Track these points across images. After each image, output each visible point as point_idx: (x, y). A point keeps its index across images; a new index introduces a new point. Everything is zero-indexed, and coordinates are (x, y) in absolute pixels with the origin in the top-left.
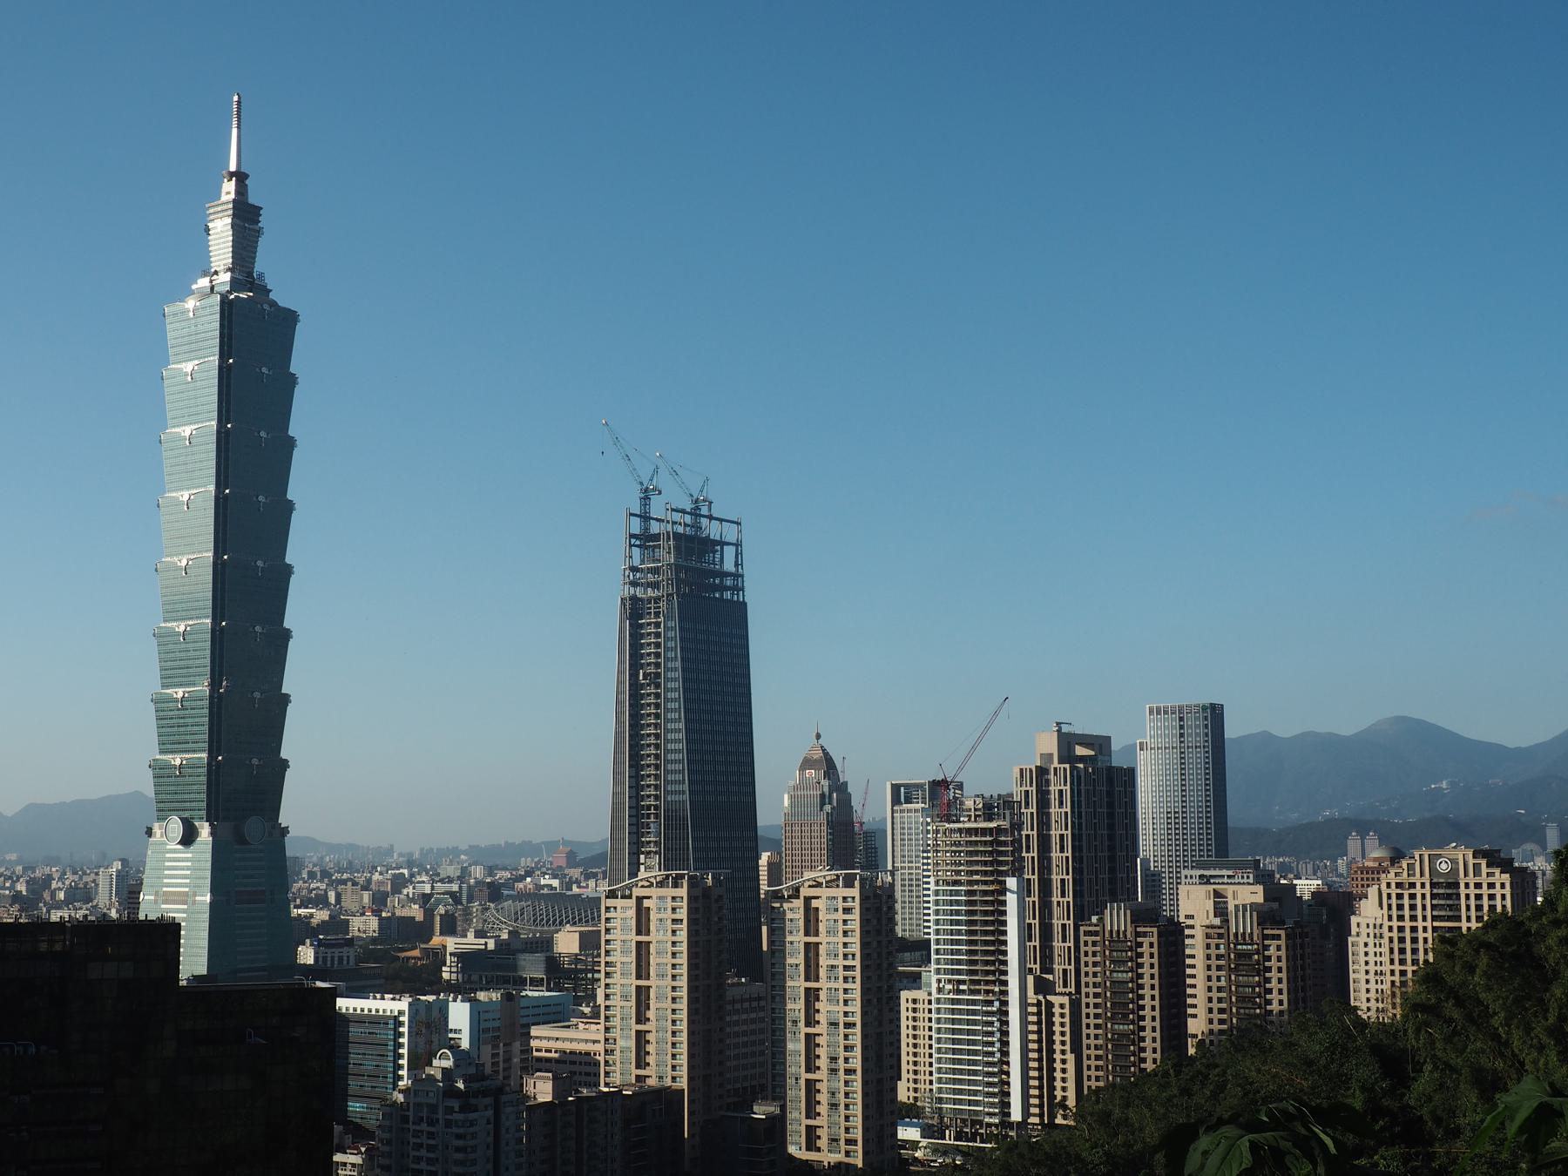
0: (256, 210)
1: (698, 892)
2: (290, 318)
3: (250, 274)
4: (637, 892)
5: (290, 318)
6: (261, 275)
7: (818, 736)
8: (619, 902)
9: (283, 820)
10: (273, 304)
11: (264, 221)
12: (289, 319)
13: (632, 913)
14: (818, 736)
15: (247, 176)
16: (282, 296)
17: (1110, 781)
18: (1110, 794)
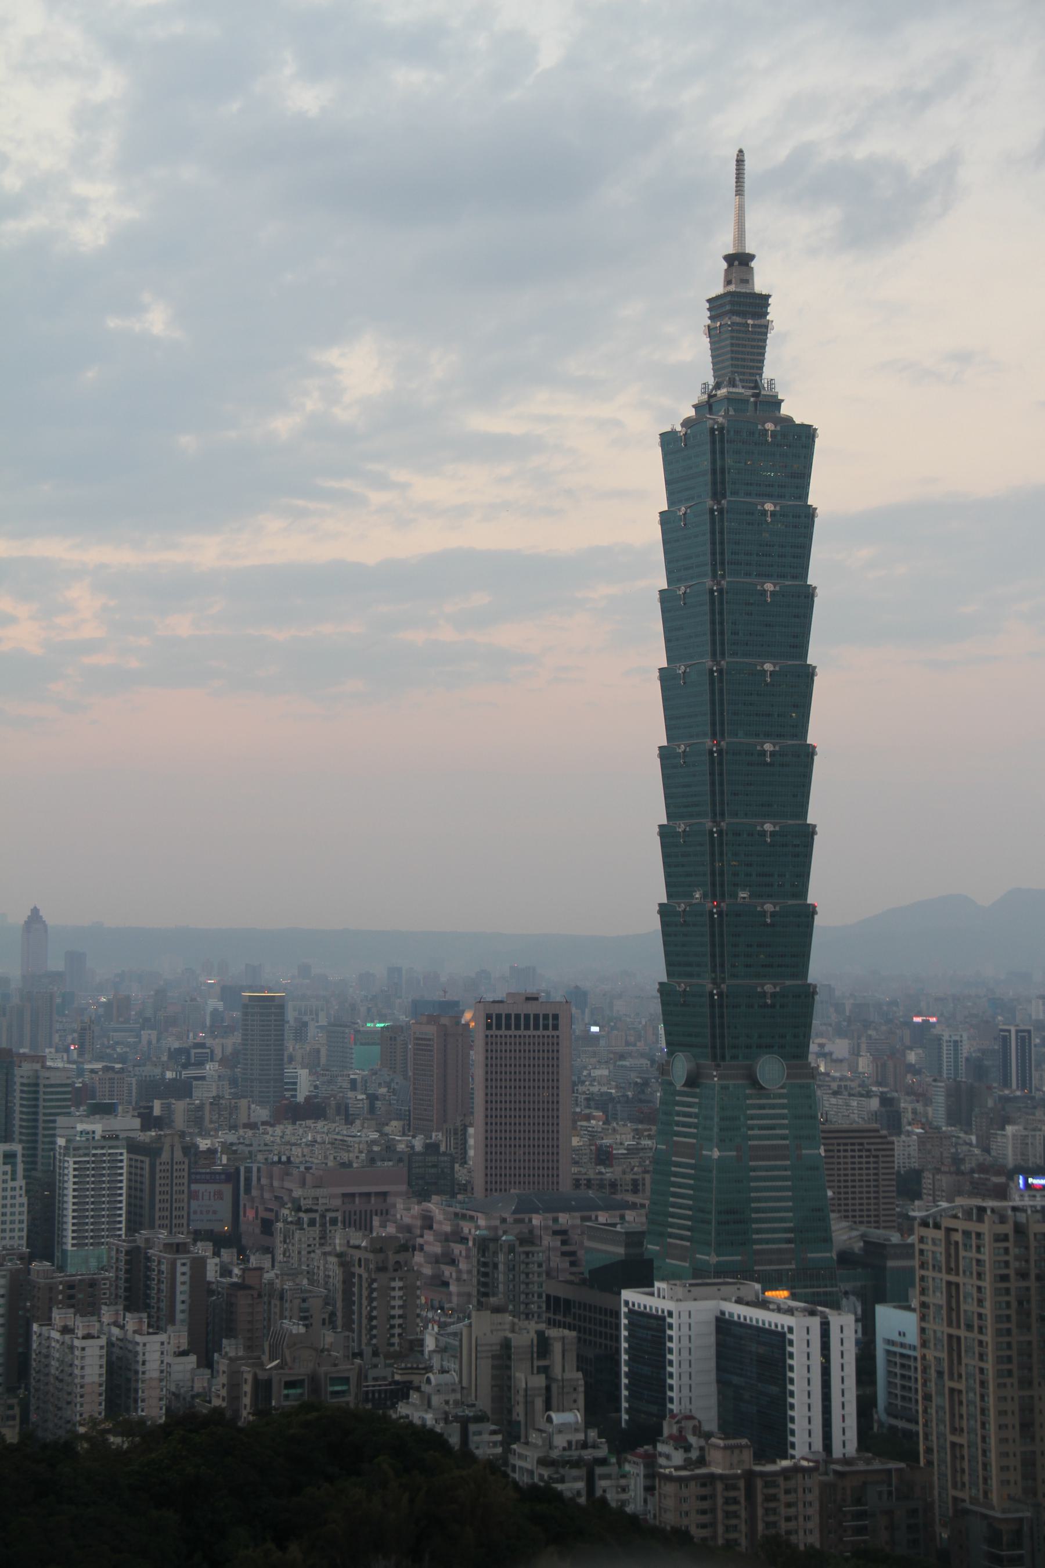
0: (763, 300)
1: (1008, 1229)
2: (805, 436)
3: (756, 385)
4: (946, 1223)
5: (805, 436)
6: (771, 382)
8: (930, 1233)
10: (789, 420)
11: (774, 313)
12: (802, 438)
13: (941, 1249)
15: (752, 257)
16: (795, 408)
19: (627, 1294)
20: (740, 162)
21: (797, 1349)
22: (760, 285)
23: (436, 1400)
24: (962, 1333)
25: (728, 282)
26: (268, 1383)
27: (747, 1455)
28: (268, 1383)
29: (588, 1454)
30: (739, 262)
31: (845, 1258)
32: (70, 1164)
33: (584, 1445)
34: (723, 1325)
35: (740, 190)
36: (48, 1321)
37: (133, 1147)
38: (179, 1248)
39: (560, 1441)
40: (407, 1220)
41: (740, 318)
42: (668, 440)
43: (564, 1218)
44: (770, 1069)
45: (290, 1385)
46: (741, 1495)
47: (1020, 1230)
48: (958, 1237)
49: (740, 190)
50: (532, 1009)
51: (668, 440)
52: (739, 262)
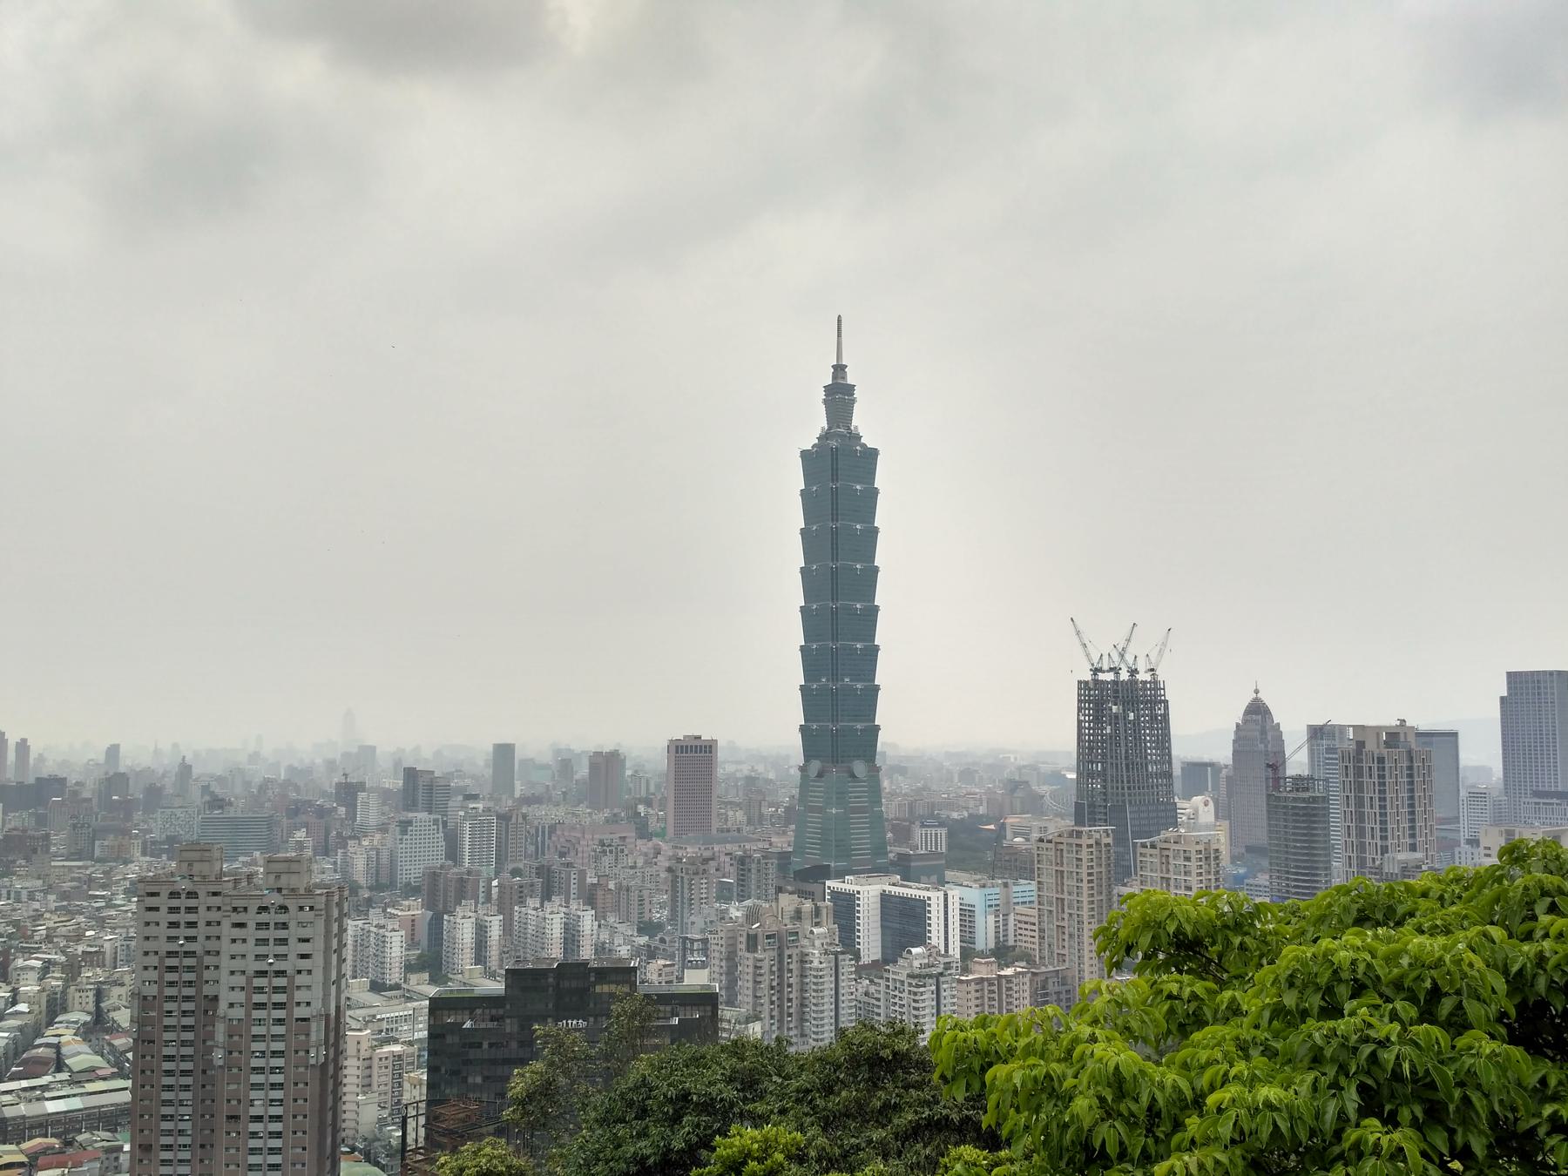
5: (873, 454)
7: (1257, 692)
8: (1044, 845)
9: (878, 762)
12: (873, 454)
14: (1257, 692)
16: (868, 440)
17: (1411, 759)
18: (1410, 768)
19: (828, 883)
20: (839, 321)
21: (933, 909)
22: (850, 381)
23: (817, 943)
24: (1065, 896)
25: (834, 377)
26: (756, 936)
27: (995, 967)
28: (756, 936)
29: (935, 971)
30: (839, 369)
31: (892, 863)
32: (467, 825)
33: (929, 966)
34: (885, 898)
35: (839, 335)
36: (522, 902)
37: (499, 817)
38: (569, 865)
39: (916, 964)
40: (644, 850)
41: (839, 396)
42: (804, 454)
43: (729, 846)
44: (859, 768)
45: (768, 937)
46: (995, 988)
47: (1098, 843)
48: (1064, 847)
49: (839, 335)
50: (697, 743)
51: (804, 454)
52: (839, 369)
